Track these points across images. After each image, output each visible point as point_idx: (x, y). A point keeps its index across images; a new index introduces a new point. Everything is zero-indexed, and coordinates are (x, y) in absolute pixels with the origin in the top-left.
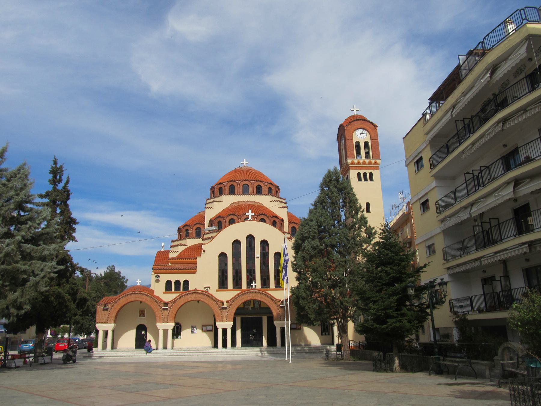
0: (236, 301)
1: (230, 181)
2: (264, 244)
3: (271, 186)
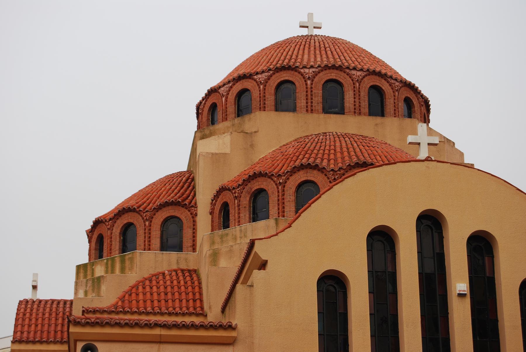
1: (278, 70)
3: (412, 96)
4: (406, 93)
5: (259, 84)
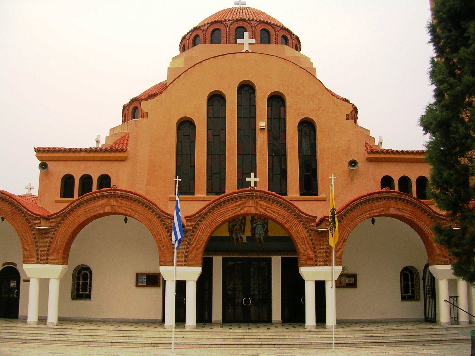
2: (277, 101)
4: (282, 33)
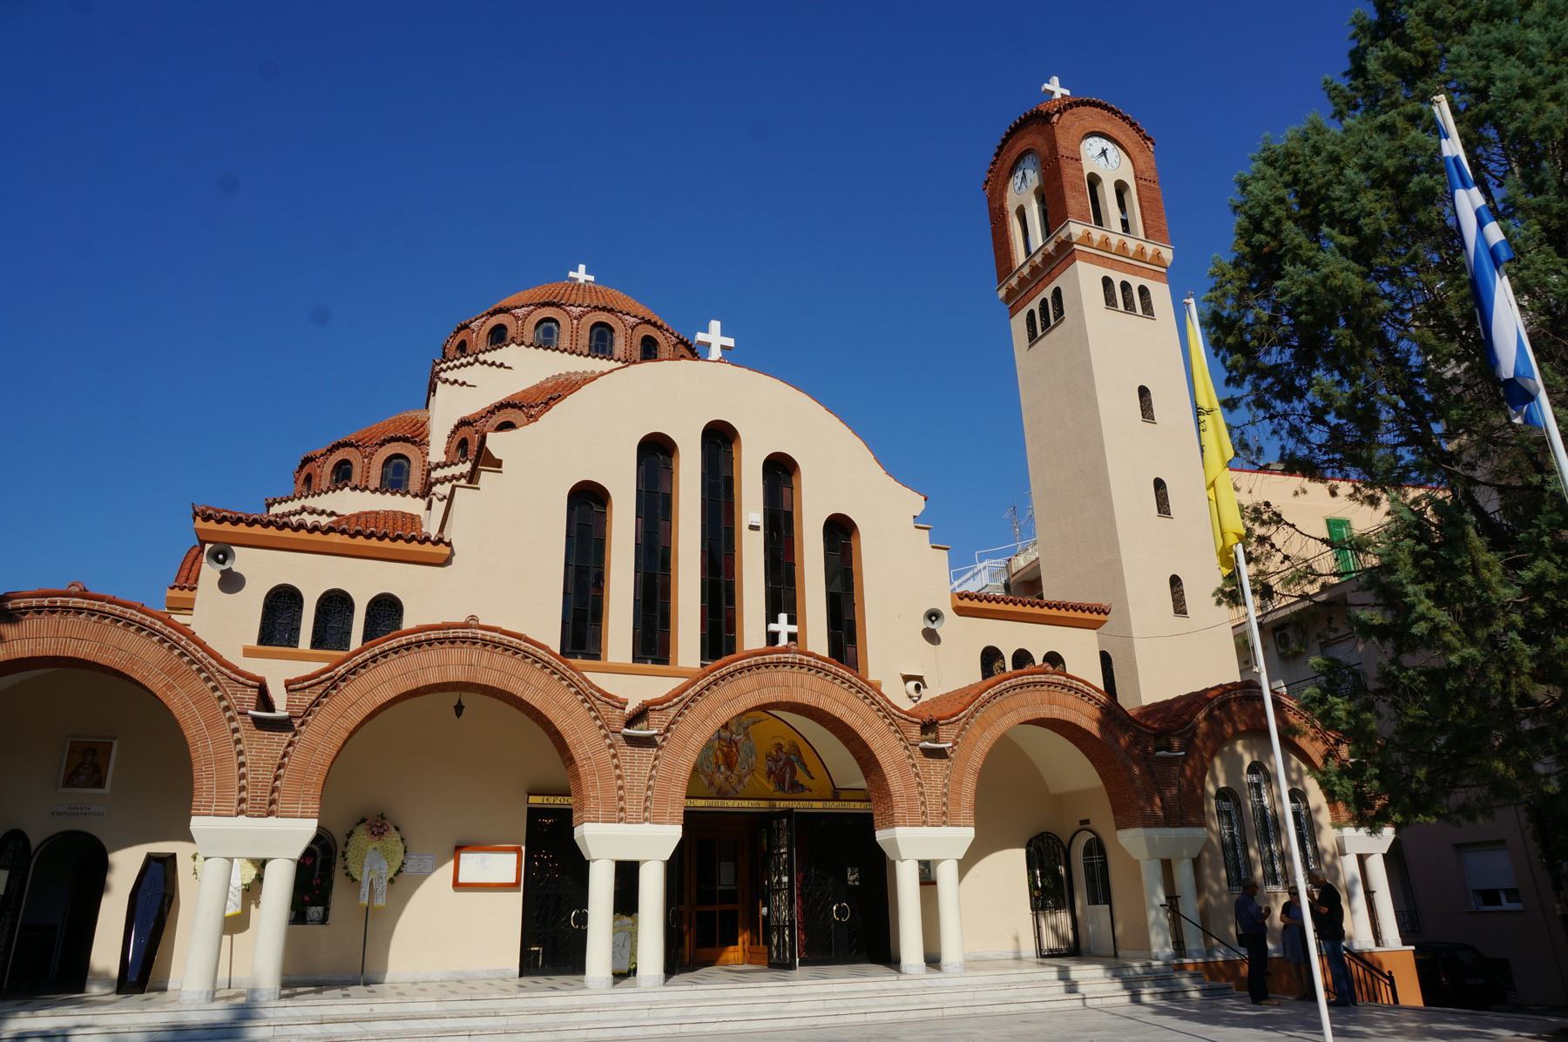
0: (703, 706)
2: (780, 470)
5: (517, 318)
